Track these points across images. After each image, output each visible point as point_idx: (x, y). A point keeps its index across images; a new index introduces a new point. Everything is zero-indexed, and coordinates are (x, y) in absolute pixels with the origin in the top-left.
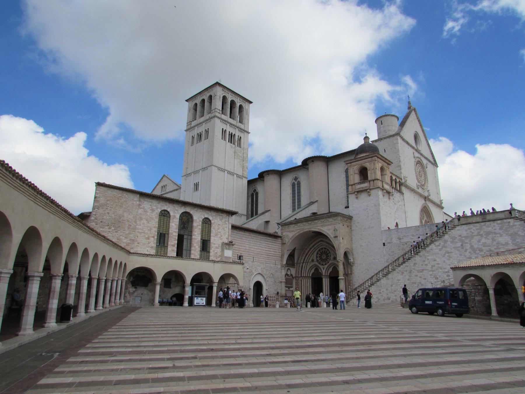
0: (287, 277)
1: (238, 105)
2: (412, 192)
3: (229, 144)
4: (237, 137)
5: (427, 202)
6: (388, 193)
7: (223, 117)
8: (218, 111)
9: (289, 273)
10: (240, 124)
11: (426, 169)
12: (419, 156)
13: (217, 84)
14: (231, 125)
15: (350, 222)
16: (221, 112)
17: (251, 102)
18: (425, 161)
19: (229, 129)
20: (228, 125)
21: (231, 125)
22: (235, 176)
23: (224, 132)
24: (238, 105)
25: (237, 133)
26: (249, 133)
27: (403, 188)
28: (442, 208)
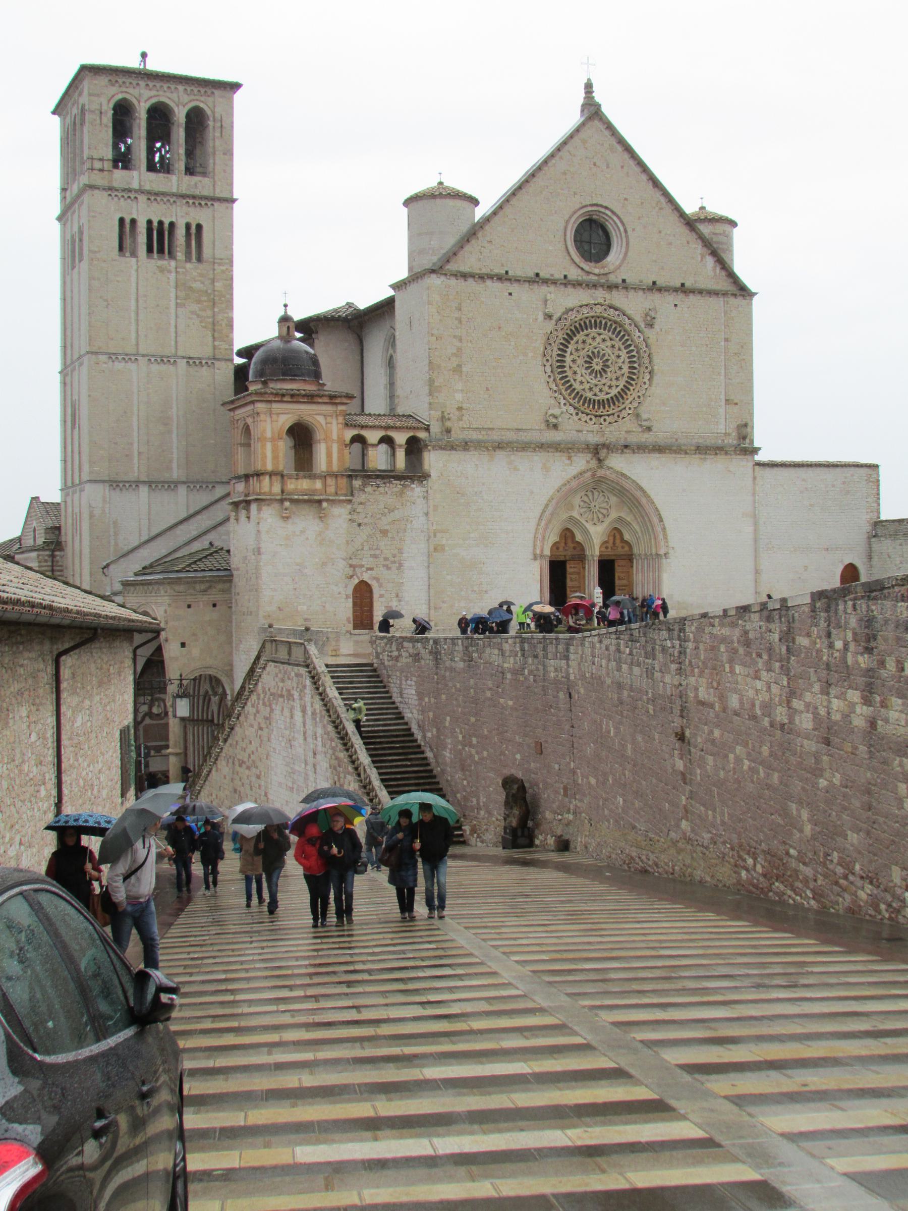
0: (148, 721)
1: (180, 115)
2: (500, 454)
3: (156, 262)
4: (180, 232)
5: (617, 462)
6: (320, 502)
7: (120, 176)
8: (98, 165)
9: (155, 710)
10: (195, 179)
11: (650, 334)
12: (600, 295)
13: (87, 71)
14: (154, 195)
15: (228, 591)
16: (108, 165)
17: (235, 87)
18: (633, 305)
19: (144, 213)
20: (142, 198)
21: (154, 195)
22: (182, 363)
23: (126, 227)
24: (180, 115)
25: (180, 215)
26: (233, 201)
27: (432, 460)
28: (755, 451)
